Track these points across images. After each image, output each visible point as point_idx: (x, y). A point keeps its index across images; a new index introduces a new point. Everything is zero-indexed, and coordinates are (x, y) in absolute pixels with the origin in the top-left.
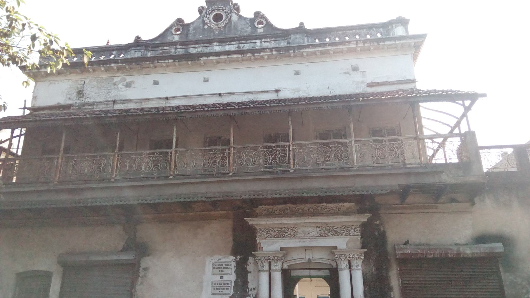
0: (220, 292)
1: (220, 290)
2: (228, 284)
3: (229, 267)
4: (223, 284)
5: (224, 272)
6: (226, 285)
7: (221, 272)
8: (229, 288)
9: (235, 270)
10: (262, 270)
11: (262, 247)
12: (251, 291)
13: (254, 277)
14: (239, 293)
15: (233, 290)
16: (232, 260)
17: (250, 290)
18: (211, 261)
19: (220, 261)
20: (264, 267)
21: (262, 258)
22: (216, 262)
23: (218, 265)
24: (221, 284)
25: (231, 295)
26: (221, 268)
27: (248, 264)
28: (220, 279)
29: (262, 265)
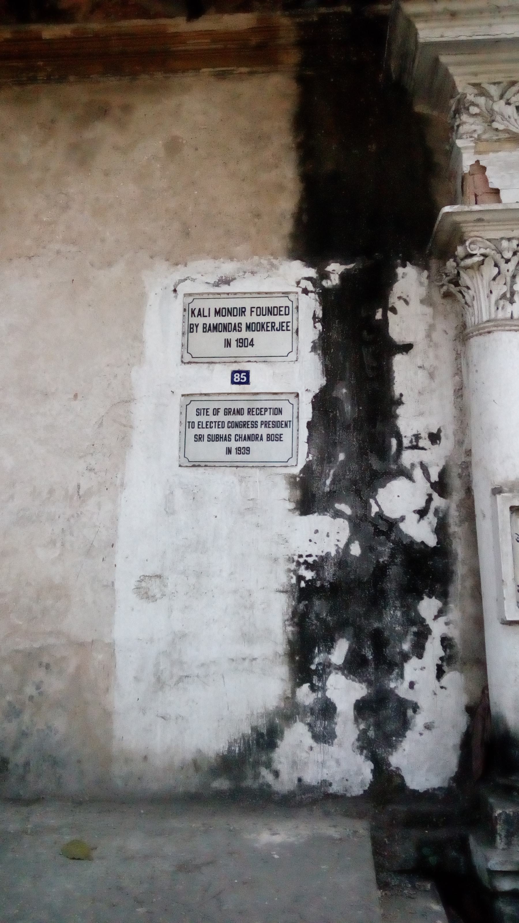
0: (234, 456)
1: (234, 445)
2: (279, 411)
3: (277, 319)
4: (250, 411)
5: (249, 351)
6: (268, 417)
7: (234, 350)
8: (286, 432)
9: (317, 337)
10: (506, 319)
11: (497, 192)
12: (415, 447)
13: (431, 376)
14: (342, 457)
15: (309, 440)
16: (298, 283)
17: (406, 442)
18: (175, 291)
19: (225, 289)
20: (512, 302)
21: (505, 243)
22: (201, 296)
23: (218, 312)
24: (239, 412)
25: (296, 471)
26: (237, 328)
27: (393, 300)
28: (233, 382)
29: (500, 289)
